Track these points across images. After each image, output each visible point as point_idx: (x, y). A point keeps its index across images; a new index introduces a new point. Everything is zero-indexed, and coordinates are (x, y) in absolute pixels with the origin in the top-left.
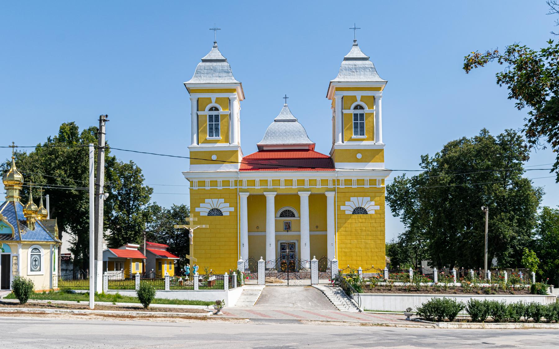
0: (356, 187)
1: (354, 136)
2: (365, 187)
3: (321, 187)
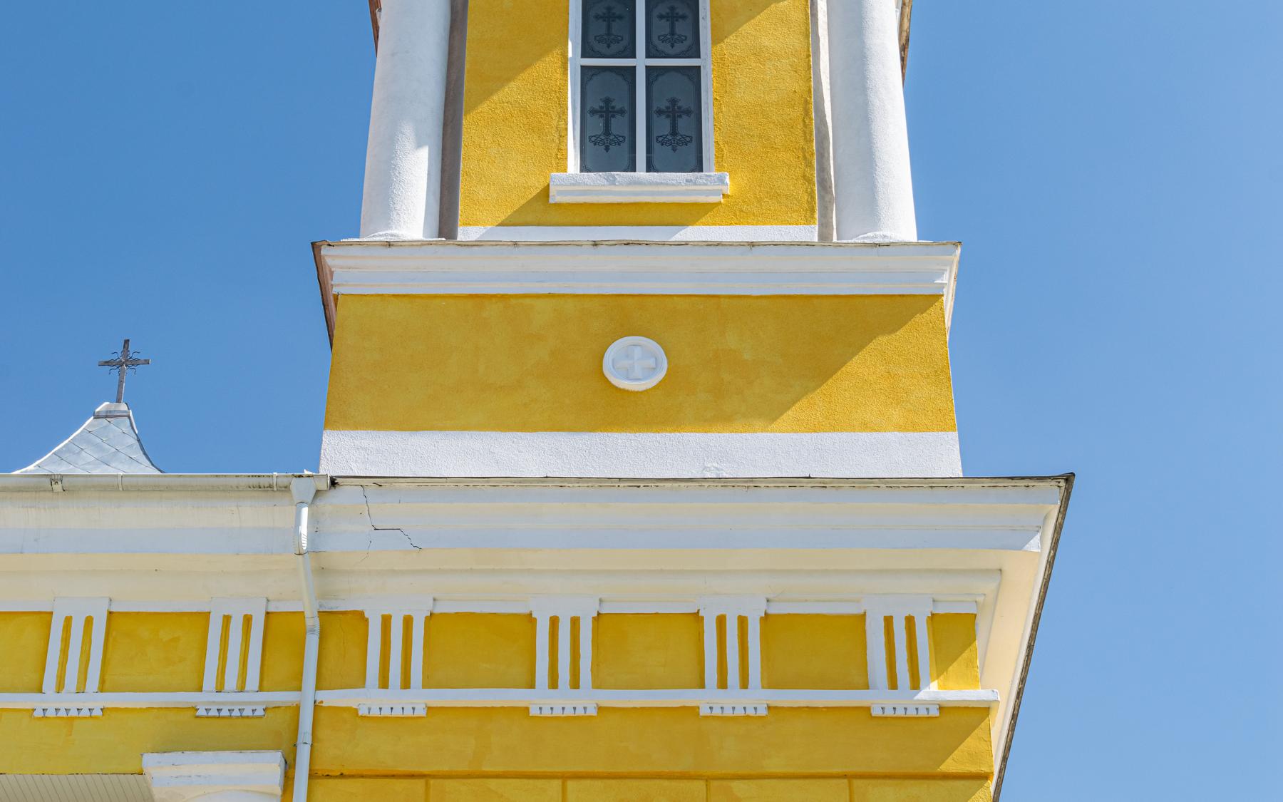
0: (586, 700)
1: (571, 175)
2: (708, 700)
3: (95, 701)
